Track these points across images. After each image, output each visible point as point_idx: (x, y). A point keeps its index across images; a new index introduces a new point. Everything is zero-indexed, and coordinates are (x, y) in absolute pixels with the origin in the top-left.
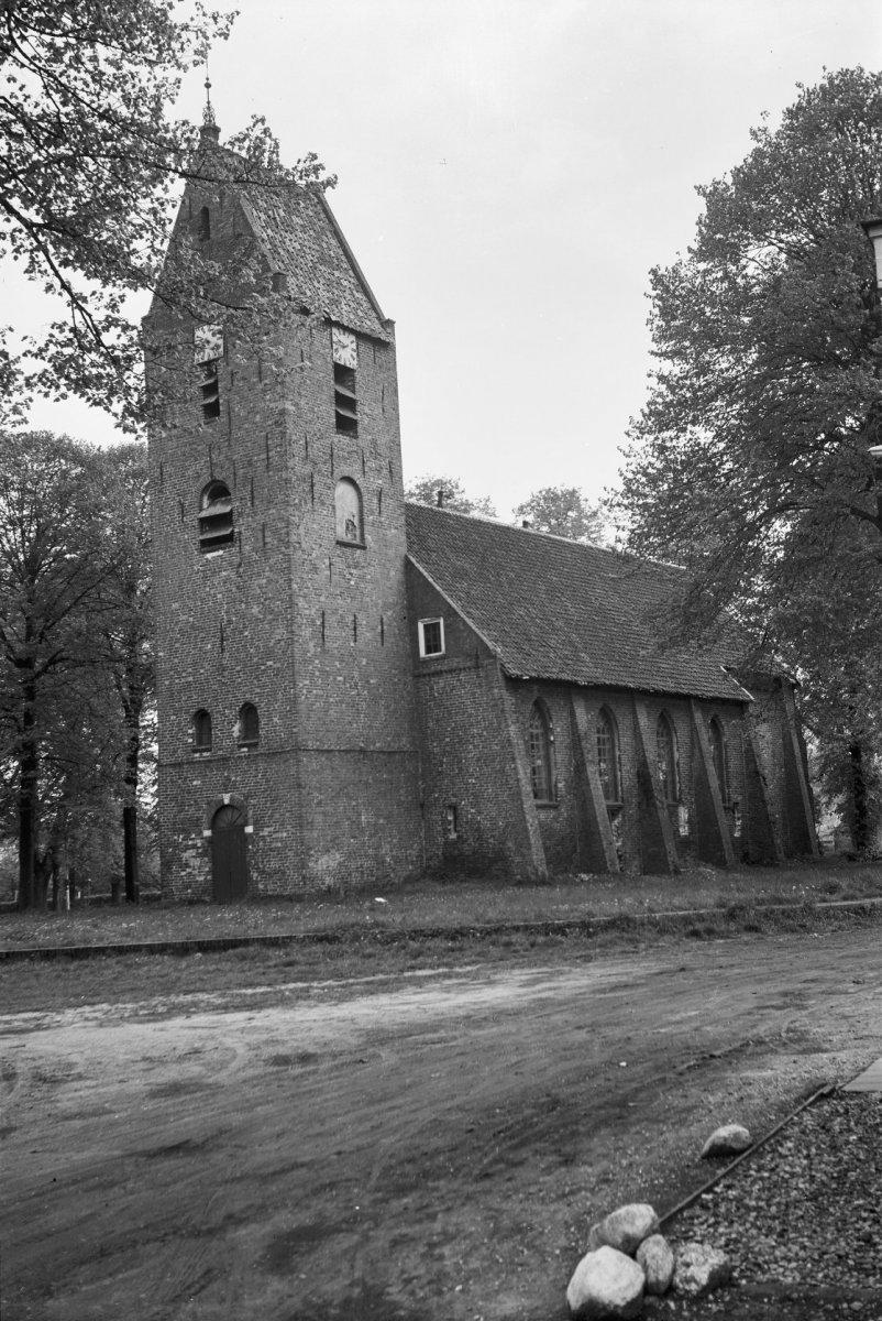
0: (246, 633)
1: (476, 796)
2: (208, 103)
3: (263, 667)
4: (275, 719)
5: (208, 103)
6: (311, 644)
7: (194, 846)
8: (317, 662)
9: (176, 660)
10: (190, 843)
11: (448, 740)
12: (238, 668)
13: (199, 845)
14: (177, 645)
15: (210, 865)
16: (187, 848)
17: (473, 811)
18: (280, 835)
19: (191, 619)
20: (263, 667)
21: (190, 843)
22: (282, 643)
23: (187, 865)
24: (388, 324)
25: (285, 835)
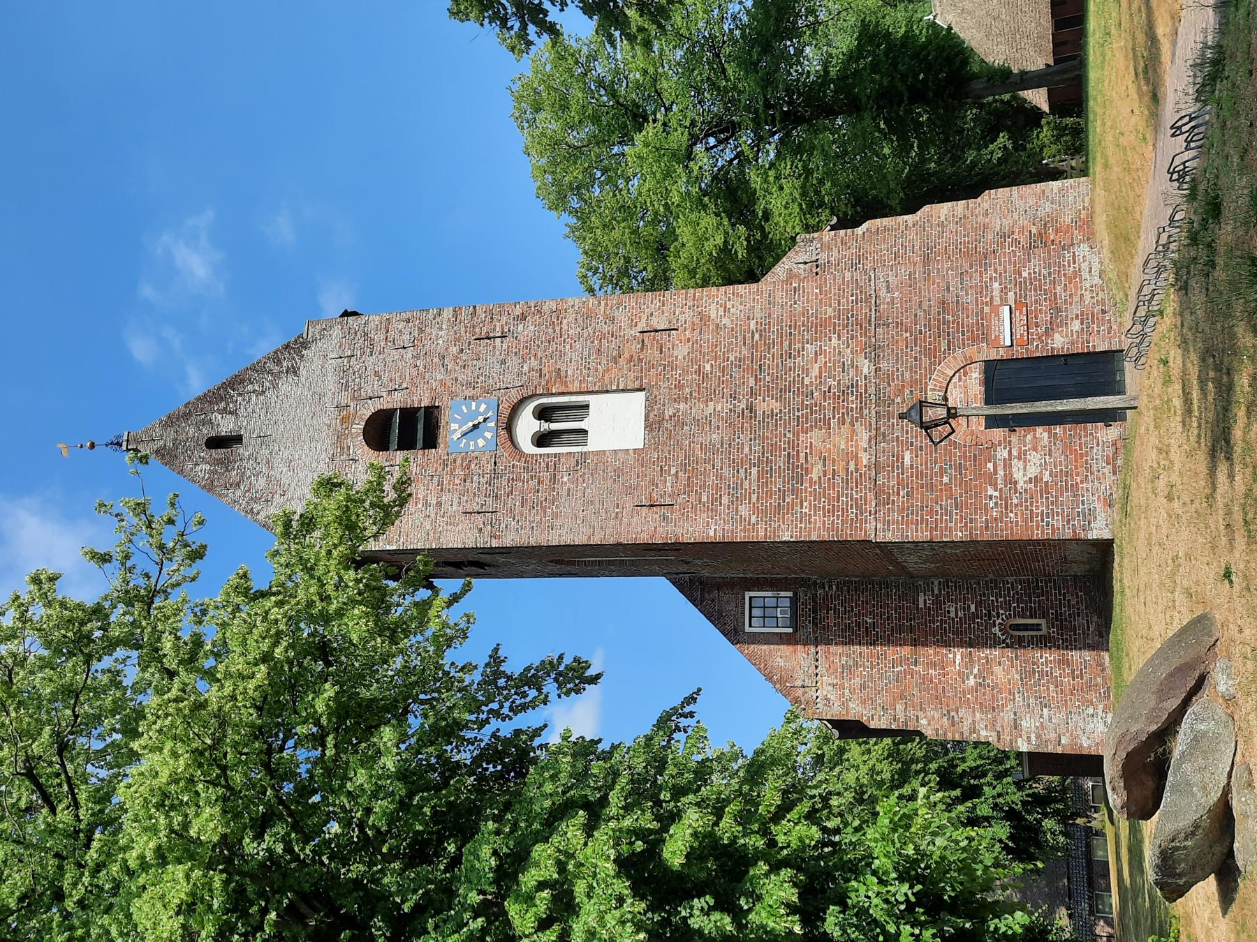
0: (708, 367)
3: (757, 336)
4: (830, 311)
7: (1007, 464)
9: (725, 500)
12: (752, 382)
13: (1006, 455)
16: (1010, 481)
18: (996, 293)
19: (673, 471)
20: (757, 336)
22: (729, 305)
23: (1036, 480)
25: (996, 285)
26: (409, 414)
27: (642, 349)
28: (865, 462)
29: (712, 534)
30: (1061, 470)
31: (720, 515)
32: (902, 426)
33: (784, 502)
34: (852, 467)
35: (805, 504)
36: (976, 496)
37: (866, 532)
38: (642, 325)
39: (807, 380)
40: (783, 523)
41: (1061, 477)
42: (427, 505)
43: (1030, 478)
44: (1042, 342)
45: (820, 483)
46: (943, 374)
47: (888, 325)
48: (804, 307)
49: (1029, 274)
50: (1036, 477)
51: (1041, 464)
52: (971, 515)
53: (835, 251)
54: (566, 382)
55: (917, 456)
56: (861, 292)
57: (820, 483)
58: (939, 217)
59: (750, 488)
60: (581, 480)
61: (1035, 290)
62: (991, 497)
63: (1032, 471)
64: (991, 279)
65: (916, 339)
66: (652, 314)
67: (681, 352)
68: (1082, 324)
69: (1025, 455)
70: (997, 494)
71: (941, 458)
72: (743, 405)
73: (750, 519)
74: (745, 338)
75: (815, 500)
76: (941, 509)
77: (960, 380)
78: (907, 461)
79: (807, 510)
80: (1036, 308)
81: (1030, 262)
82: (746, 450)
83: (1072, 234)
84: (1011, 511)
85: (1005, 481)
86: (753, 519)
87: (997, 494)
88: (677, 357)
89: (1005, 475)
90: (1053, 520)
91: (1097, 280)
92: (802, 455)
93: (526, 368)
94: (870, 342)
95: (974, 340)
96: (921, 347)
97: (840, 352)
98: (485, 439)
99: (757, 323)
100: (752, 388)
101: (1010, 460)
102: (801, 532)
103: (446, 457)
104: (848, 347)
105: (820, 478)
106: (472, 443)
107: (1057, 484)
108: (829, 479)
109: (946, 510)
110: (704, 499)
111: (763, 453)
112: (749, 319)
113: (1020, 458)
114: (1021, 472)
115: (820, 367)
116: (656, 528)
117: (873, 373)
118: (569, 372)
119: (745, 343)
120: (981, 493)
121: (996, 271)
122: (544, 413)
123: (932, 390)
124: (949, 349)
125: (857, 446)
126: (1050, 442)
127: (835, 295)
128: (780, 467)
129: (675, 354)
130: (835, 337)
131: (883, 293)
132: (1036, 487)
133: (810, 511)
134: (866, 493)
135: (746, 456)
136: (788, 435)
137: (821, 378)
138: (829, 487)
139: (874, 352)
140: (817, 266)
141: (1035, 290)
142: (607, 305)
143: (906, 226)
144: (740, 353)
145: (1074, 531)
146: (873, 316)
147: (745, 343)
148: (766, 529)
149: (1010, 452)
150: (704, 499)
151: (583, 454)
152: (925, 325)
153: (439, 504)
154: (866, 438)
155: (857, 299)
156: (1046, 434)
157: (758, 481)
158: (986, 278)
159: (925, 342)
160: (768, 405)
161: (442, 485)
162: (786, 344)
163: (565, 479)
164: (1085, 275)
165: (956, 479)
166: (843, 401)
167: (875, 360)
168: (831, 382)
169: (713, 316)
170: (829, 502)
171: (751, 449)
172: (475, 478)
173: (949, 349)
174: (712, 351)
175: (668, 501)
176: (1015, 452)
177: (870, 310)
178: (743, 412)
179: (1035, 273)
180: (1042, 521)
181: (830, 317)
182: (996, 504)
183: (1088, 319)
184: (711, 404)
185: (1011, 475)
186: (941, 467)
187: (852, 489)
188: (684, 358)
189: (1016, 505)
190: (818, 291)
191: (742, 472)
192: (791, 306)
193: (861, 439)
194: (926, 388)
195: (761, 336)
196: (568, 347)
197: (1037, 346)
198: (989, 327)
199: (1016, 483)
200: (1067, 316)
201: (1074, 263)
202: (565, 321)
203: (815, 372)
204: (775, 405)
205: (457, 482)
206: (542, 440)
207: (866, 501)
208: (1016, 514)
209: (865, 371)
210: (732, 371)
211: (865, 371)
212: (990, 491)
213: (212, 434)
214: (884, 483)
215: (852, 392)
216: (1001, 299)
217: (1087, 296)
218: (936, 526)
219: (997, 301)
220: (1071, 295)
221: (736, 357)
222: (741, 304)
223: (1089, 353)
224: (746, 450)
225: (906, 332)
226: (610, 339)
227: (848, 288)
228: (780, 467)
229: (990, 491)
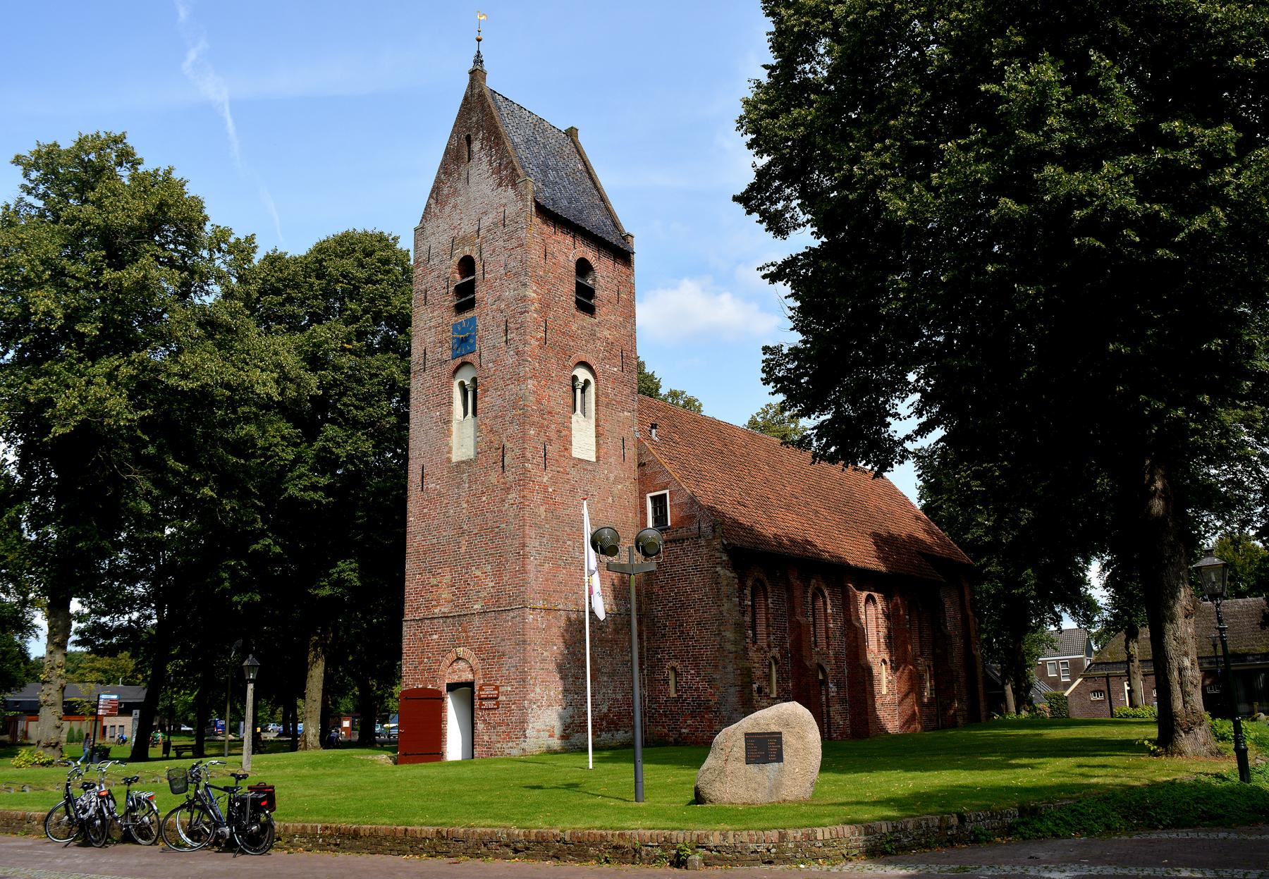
0: (484, 499)
1: (696, 658)
2: (479, 52)
5: (479, 52)
6: (542, 509)
8: (547, 526)
11: (671, 604)
14: (425, 510)
17: (693, 672)
22: (515, 506)
24: (626, 238)
25: (509, 689)
29: (411, 519)
34: (434, 603)
38: (508, 445)
53: (705, 551)
61: (505, 713)
72: (465, 527)
78: (435, 637)
82: (444, 534)
91: (507, 751)
92: (440, 571)
93: (491, 365)
95: (485, 676)
125: (442, 605)
130: (492, 584)
131: (512, 614)
141: (505, 713)
154: (446, 610)
158: (514, 682)
163: (438, 413)
164: (510, 744)
169: (510, 497)
183: (489, 745)
191: (435, 533)
196: (499, 393)
198: (490, 685)
203: (478, 573)
204: (463, 550)
209: (475, 607)
211: (475, 607)
217: (499, 745)
220: (500, 735)
224: (444, 534)
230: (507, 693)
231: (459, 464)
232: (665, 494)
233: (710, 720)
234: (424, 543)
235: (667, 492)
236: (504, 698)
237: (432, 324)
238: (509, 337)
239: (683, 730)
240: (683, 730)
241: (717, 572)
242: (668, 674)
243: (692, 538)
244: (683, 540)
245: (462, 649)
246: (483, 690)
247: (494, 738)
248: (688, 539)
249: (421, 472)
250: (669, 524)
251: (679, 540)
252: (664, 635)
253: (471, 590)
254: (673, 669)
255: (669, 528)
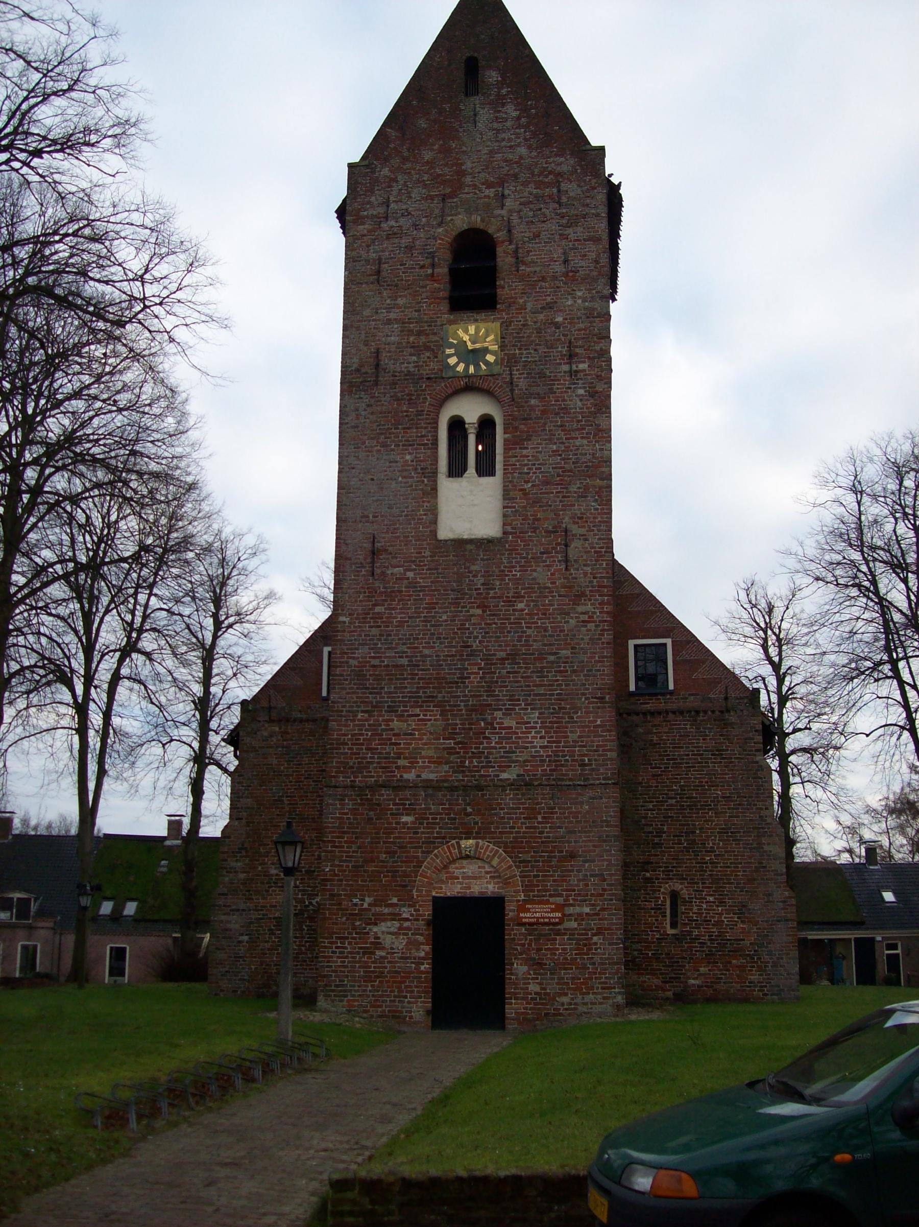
0: (521, 606)
3: (552, 658)
7: (395, 917)
9: (374, 631)
10: (386, 911)
13: (405, 916)
15: (427, 948)
17: (711, 899)
18: (578, 910)
19: (410, 574)
20: (552, 658)
21: (386, 911)
23: (378, 945)
25: (587, 910)
26: (489, 276)
27: (547, 532)
28: (406, 776)
30: (386, 968)
31: (360, 627)
32: (441, 814)
33: (371, 693)
34: (401, 762)
35: (366, 715)
36: (363, 886)
37: (334, 777)
38: (575, 529)
39: (498, 714)
40: (348, 693)
41: (379, 967)
42: (389, 309)
43: (379, 938)
44: (521, 954)
45: (387, 730)
46: (494, 855)
47: (552, 799)
48: (580, 708)
49: (596, 944)
50: (380, 943)
51: (392, 948)
52: (346, 880)
54: (515, 449)
55: (408, 828)
56: (593, 770)
57: (387, 730)
58: (768, 844)
59: (386, 657)
60: (405, 474)
62: (363, 900)
63: (388, 941)
64: (593, 905)
65: (535, 828)
66: (586, 540)
67: (541, 575)
68: (536, 993)
69: (404, 934)
70: (366, 906)
71: (404, 852)
72: (475, 645)
73: (354, 658)
74: (551, 645)
75: (369, 725)
76: (354, 852)
77: (487, 873)
78: (405, 819)
79: (359, 717)
80: (558, 949)
81: (610, 944)
83: (738, 983)
84: (347, 919)
85: (378, 914)
86: (353, 662)
87: (366, 906)
88: (535, 571)
89: (384, 914)
90: (338, 957)
91: (581, 1009)
92: (417, 711)
93: (533, 402)
94: (536, 780)
95: (527, 888)
96: (524, 833)
97: (527, 748)
98: (457, 364)
99: (568, 658)
100: (494, 655)
101: (400, 920)
102: (337, 711)
103: (439, 323)
104: (532, 756)
105: (392, 730)
106: (452, 351)
107: (373, 962)
108: (391, 739)
109: (351, 856)
110: (378, 609)
111: (423, 670)
112: (573, 648)
113: (400, 928)
114: (384, 929)
115: (511, 728)
116: (350, 559)
117: (500, 783)
118: (525, 452)
119: (545, 645)
120: (367, 890)
121: (603, 909)
122: (486, 424)
123: (477, 844)
124: (520, 862)
126: (415, 958)
127: (593, 741)
128: (406, 688)
129: (538, 569)
132: (372, 943)
133: (359, 720)
134: (373, 777)
135: (421, 652)
136: (440, 695)
137: (500, 728)
138: (383, 739)
139: (523, 785)
140: (722, 712)
142: (600, 488)
143: (761, 809)
144: (535, 641)
145: (325, 976)
146: (563, 783)
147: (545, 645)
148: (342, 675)
149: (407, 920)
150: (378, 609)
151: (435, 473)
152: (549, 837)
153: (389, 322)
154: (432, 776)
155: (585, 765)
156: (422, 954)
157: (393, 666)
159: (531, 837)
160: (475, 673)
161: (410, 323)
162: (542, 691)
163: (408, 457)
165: (382, 867)
166: (473, 753)
167: (514, 785)
168: (495, 739)
169: (580, 609)
170: (369, 740)
171: (426, 656)
172: (414, 358)
173: (520, 862)
174: (539, 610)
175: (378, 571)
176: (406, 924)
177: (570, 780)
178: (468, 646)
179: (596, 949)
180: (337, 947)
181: (567, 737)
182: (356, 905)
184: (479, 611)
185: (385, 920)
186: (396, 852)
187: (379, 763)
188: (534, 579)
189: (353, 924)
190: (599, 723)
191: (404, 648)
192: (583, 694)
193: (432, 772)
194: (480, 838)
195: (552, 662)
197: (517, 949)
198: (541, 902)
199: (376, 924)
200: (546, 979)
201: (603, 988)
202: (585, 442)
203: (507, 722)
205: (411, 339)
206: (457, 425)
207: (366, 777)
208: (344, 924)
209: (504, 776)
210: (515, 632)
212: (368, 900)
213: (482, 63)
214: (383, 795)
215: (482, 762)
216: (570, 915)
217: (565, 1000)
218: (336, 847)
219: (570, 910)
221: (530, 636)
222: (590, 639)
223: (504, 998)
224: (426, 652)
225: (543, 818)
226: (560, 495)
227: (599, 755)
228: (406, 688)
229: (368, 900)
230: (579, 917)
231: (460, 544)
232: (665, 645)
233: (742, 968)
234: (376, 662)
235: (668, 642)
236: (574, 925)
237: (392, 316)
238: (574, 367)
239: (693, 982)
240: (693, 982)
241: (757, 762)
242: (664, 901)
243: (713, 712)
244: (697, 712)
245: (471, 842)
246: (528, 910)
247: (552, 987)
248: (705, 712)
249: (368, 546)
250: (671, 687)
251: (690, 711)
252: (659, 845)
253: (495, 748)
254: (674, 895)
255: (671, 693)
